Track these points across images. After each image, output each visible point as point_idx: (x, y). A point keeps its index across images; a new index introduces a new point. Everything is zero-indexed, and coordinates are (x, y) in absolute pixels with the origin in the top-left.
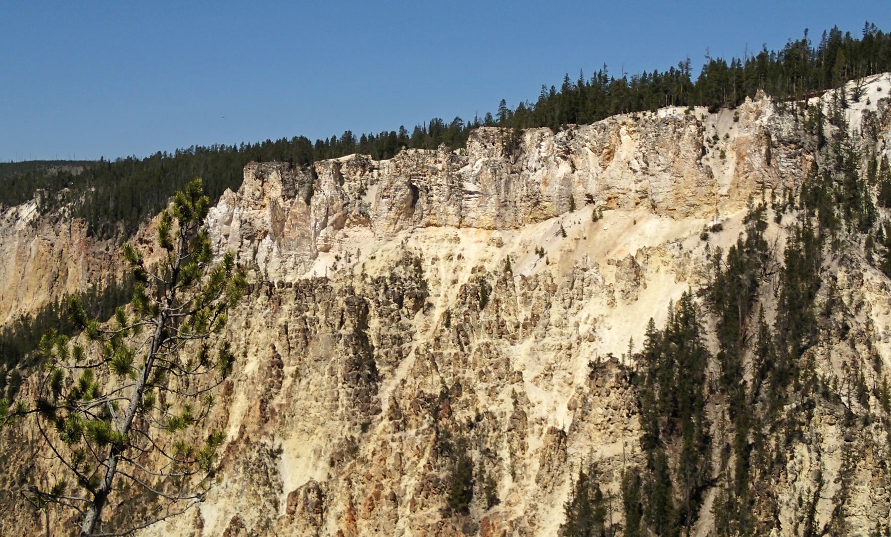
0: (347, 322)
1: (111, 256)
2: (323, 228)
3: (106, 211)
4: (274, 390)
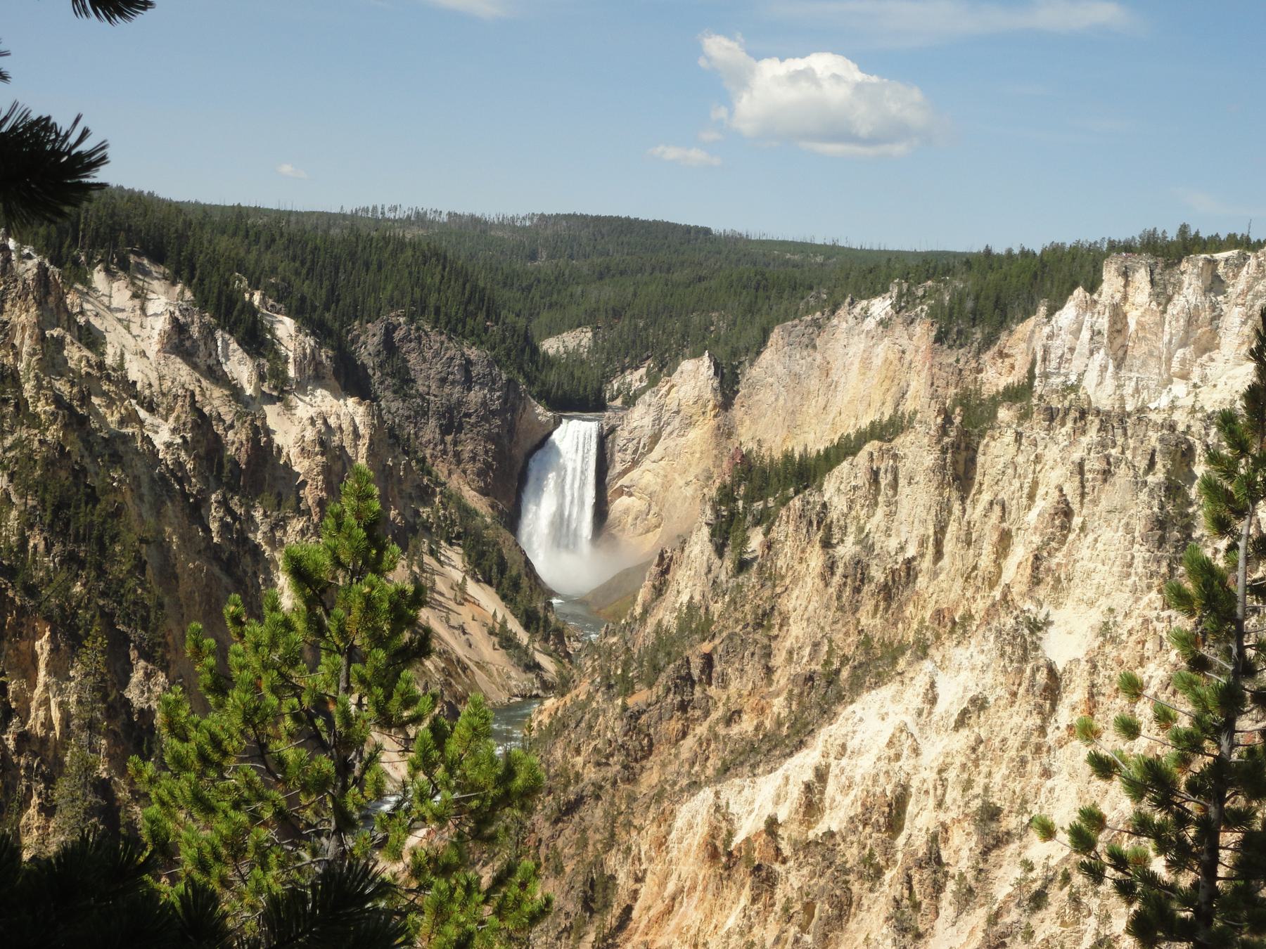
0: (1159, 466)
1: (961, 370)
2: (1181, 347)
3: (961, 313)
4: (1053, 544)
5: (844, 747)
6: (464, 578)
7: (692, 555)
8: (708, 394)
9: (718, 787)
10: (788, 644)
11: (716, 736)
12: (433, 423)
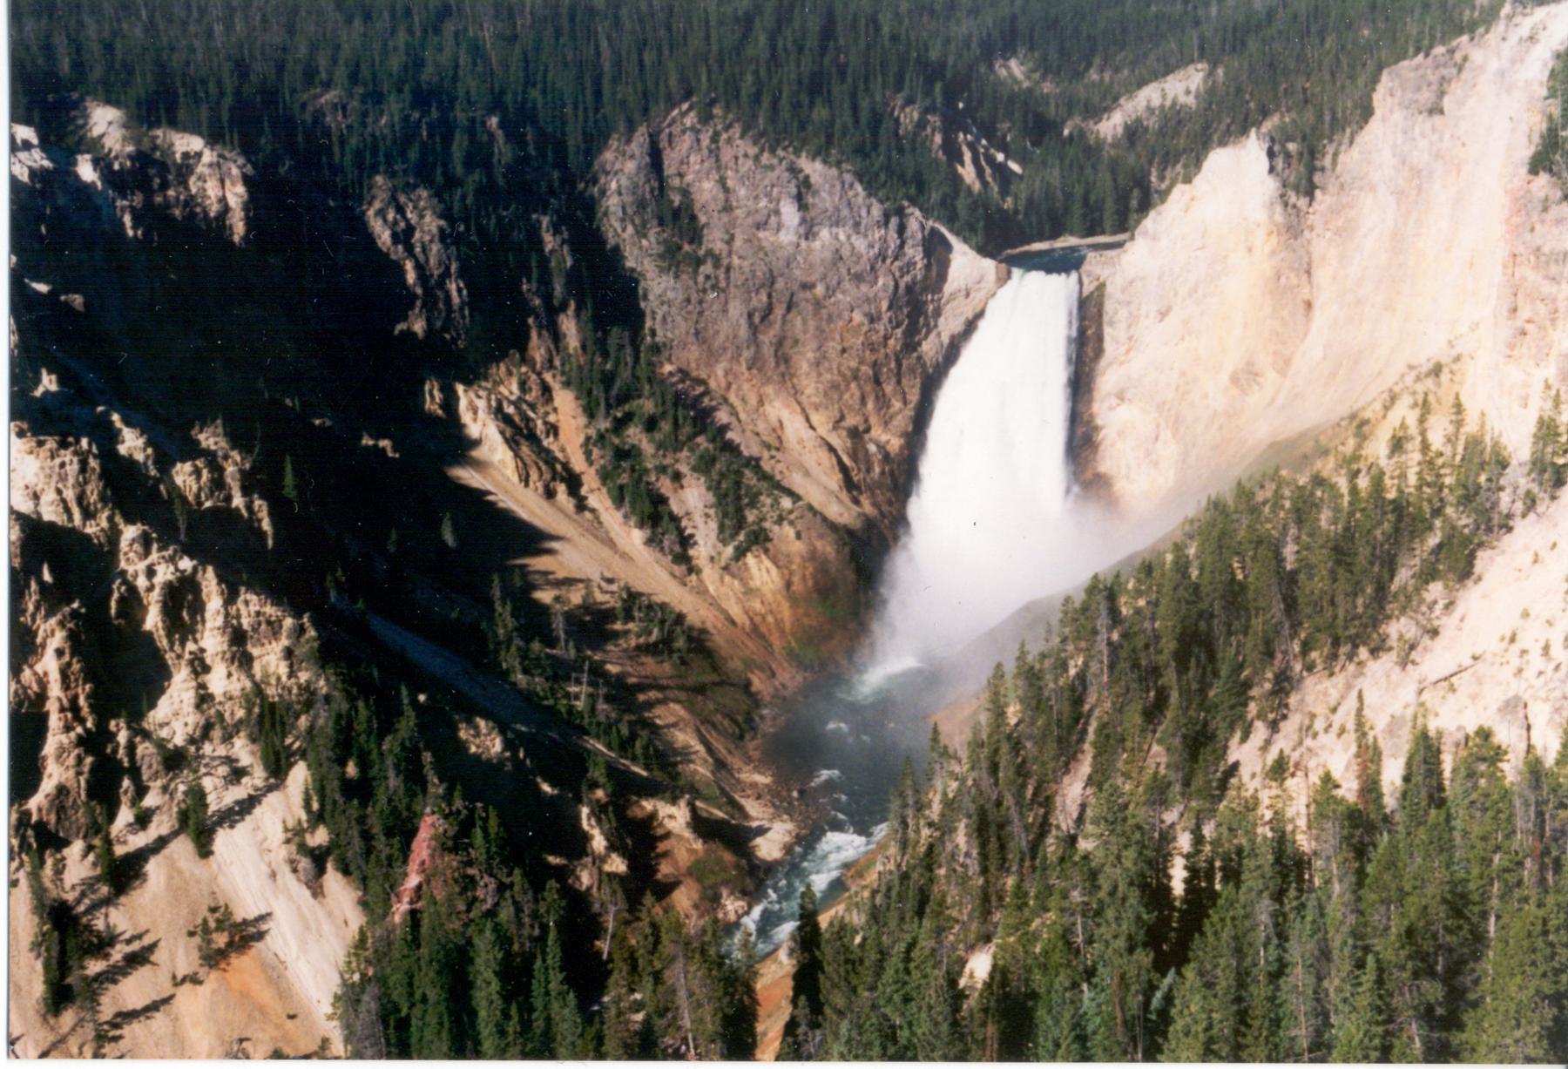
12: (736, 309)
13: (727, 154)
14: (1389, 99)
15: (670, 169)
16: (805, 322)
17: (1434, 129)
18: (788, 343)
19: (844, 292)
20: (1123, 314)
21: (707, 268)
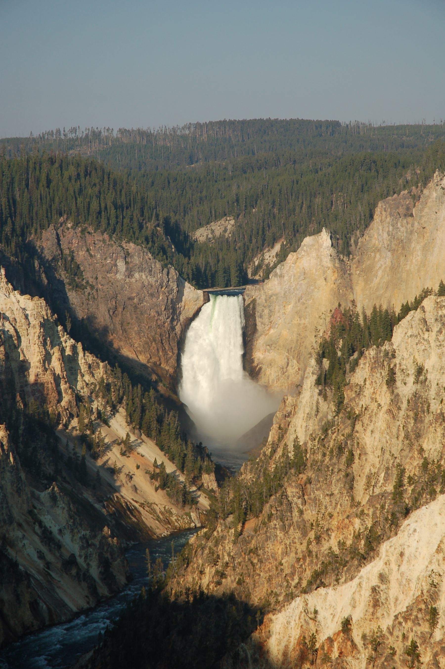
5: (402, 554)
6: (128, 435)
7: (304, 401)
8: (327, 262)
9: (307, 596)
10: (367, 471)
11: (310, 552)
13: (89, 239)
14: (384, 213)
15: (64, 246)
16: (131, 315)
17: (407, 223)
18: (125, 324)
19: (146, 302)
20: (266, 311)
21: (88, 290)
